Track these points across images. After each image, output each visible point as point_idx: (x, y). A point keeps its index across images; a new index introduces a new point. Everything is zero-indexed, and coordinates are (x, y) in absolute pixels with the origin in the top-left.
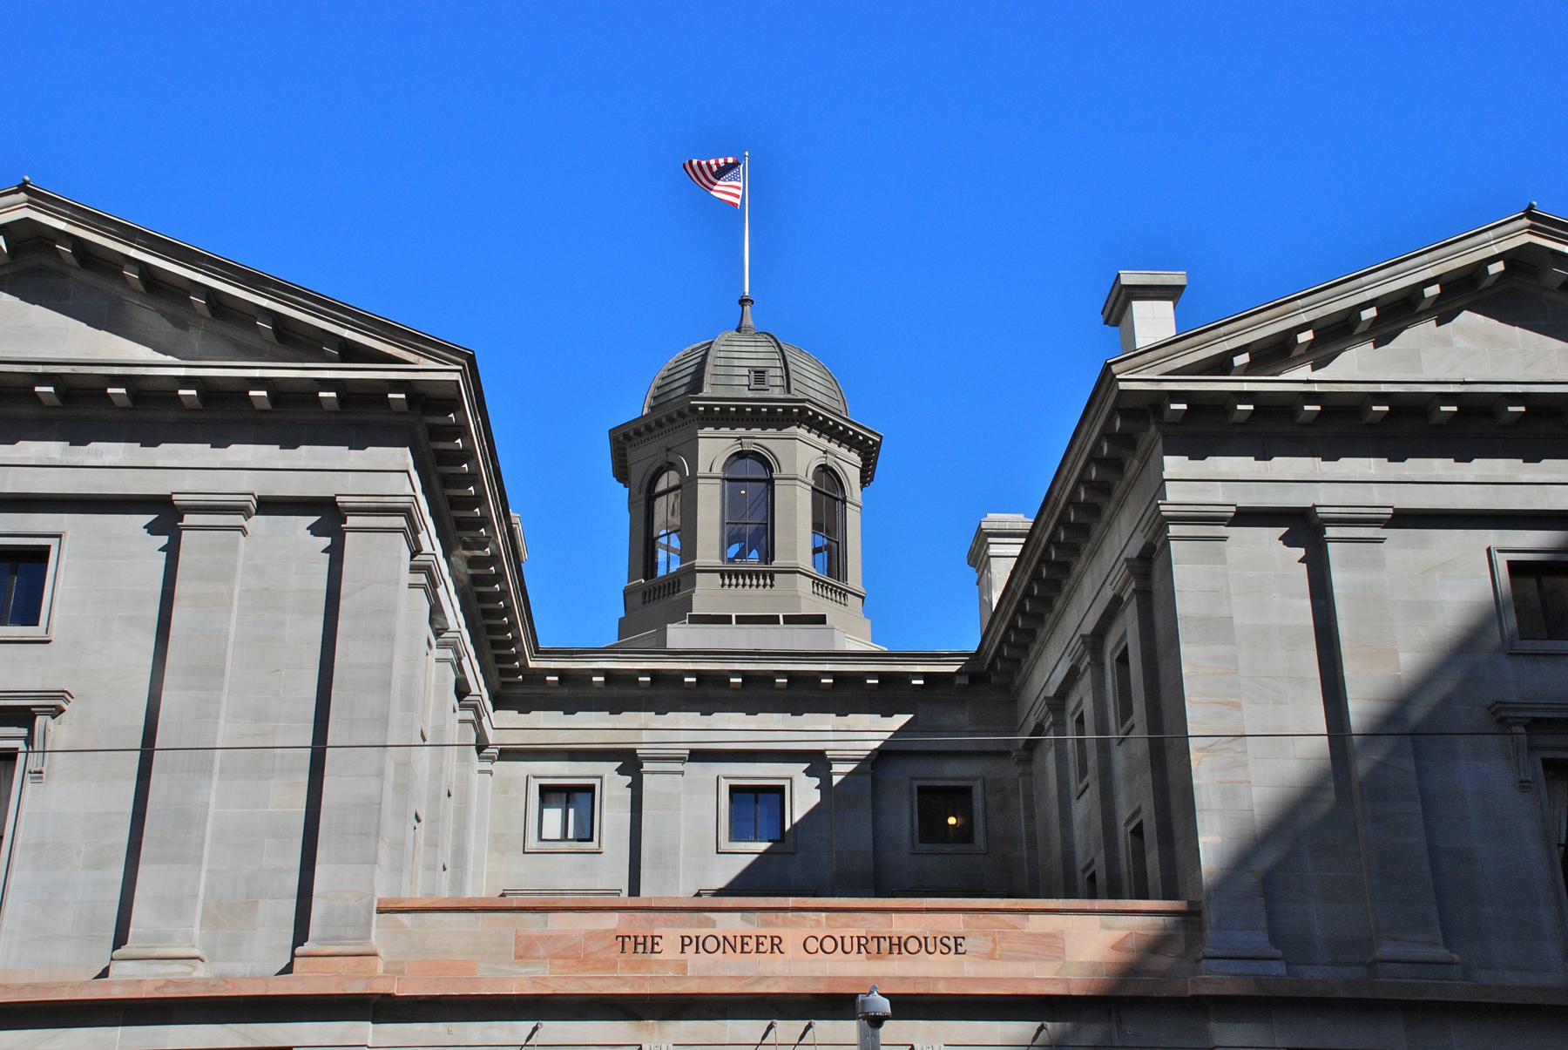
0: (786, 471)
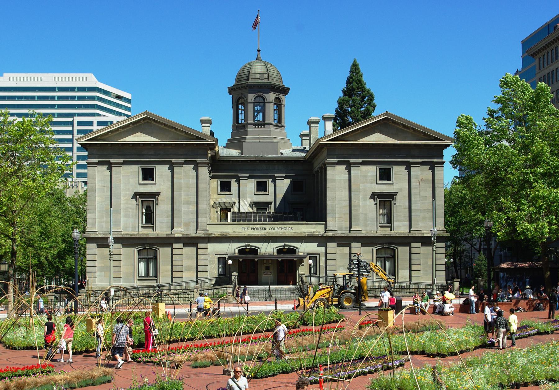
0: (268, 101)
